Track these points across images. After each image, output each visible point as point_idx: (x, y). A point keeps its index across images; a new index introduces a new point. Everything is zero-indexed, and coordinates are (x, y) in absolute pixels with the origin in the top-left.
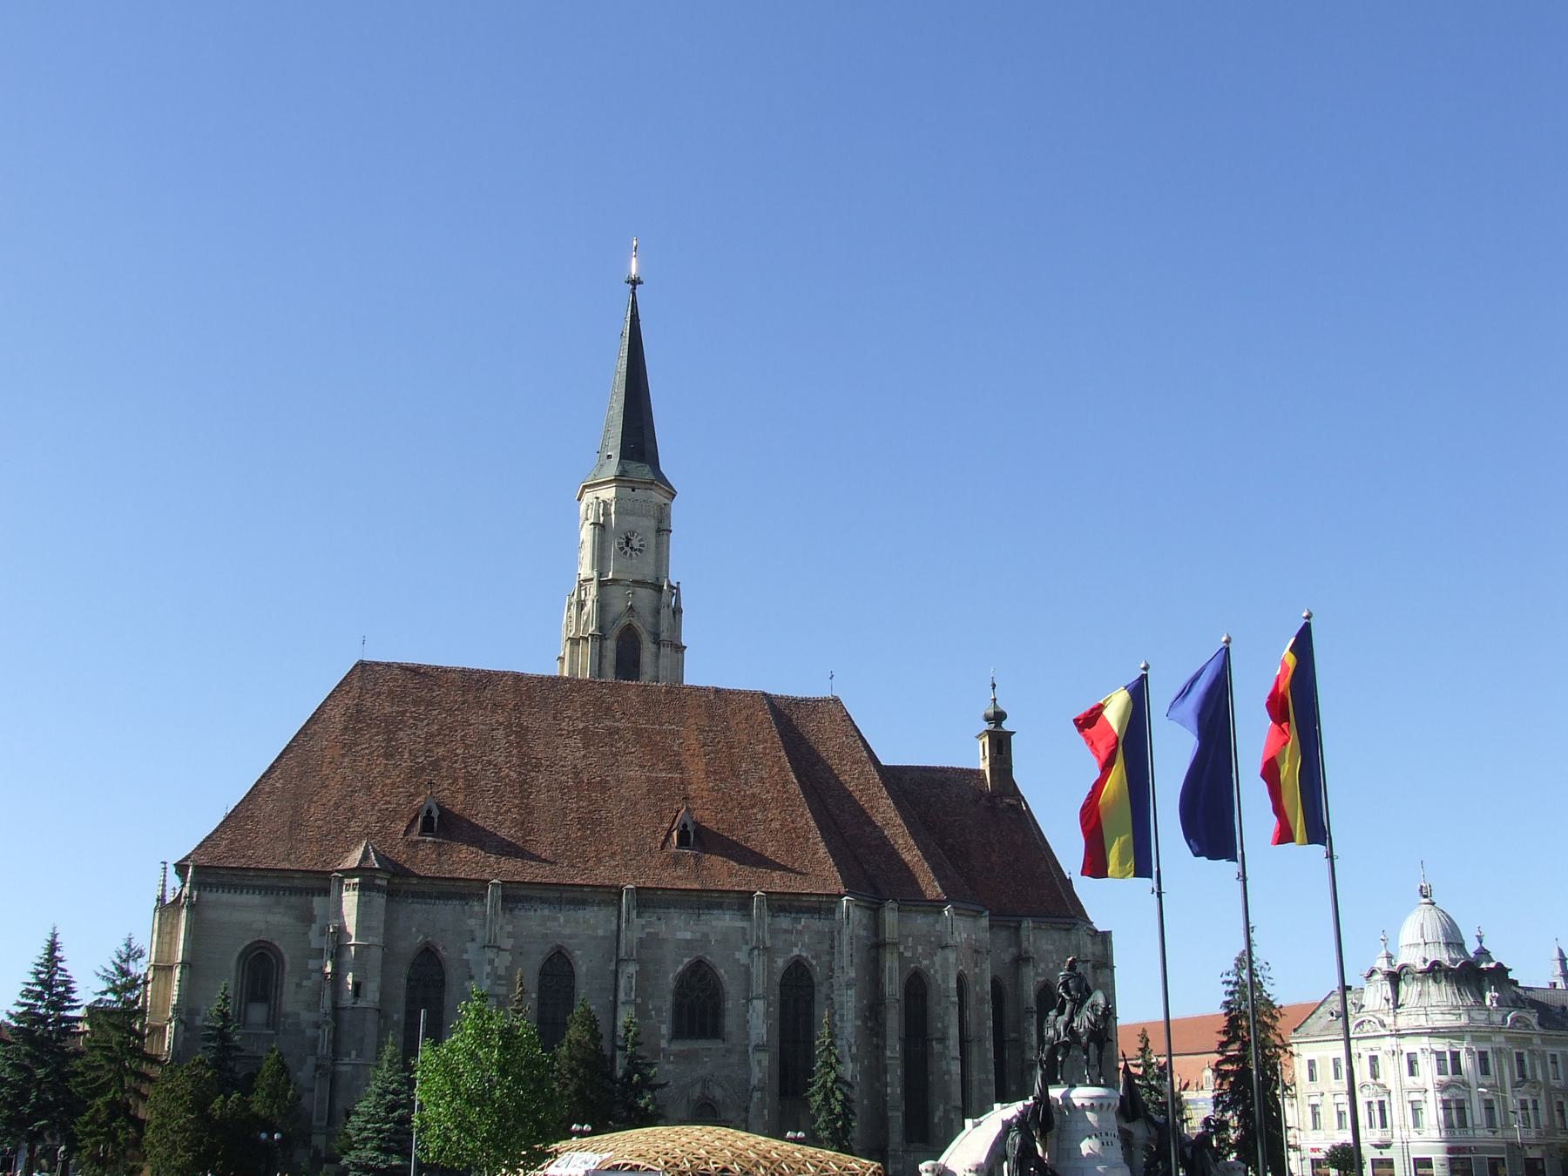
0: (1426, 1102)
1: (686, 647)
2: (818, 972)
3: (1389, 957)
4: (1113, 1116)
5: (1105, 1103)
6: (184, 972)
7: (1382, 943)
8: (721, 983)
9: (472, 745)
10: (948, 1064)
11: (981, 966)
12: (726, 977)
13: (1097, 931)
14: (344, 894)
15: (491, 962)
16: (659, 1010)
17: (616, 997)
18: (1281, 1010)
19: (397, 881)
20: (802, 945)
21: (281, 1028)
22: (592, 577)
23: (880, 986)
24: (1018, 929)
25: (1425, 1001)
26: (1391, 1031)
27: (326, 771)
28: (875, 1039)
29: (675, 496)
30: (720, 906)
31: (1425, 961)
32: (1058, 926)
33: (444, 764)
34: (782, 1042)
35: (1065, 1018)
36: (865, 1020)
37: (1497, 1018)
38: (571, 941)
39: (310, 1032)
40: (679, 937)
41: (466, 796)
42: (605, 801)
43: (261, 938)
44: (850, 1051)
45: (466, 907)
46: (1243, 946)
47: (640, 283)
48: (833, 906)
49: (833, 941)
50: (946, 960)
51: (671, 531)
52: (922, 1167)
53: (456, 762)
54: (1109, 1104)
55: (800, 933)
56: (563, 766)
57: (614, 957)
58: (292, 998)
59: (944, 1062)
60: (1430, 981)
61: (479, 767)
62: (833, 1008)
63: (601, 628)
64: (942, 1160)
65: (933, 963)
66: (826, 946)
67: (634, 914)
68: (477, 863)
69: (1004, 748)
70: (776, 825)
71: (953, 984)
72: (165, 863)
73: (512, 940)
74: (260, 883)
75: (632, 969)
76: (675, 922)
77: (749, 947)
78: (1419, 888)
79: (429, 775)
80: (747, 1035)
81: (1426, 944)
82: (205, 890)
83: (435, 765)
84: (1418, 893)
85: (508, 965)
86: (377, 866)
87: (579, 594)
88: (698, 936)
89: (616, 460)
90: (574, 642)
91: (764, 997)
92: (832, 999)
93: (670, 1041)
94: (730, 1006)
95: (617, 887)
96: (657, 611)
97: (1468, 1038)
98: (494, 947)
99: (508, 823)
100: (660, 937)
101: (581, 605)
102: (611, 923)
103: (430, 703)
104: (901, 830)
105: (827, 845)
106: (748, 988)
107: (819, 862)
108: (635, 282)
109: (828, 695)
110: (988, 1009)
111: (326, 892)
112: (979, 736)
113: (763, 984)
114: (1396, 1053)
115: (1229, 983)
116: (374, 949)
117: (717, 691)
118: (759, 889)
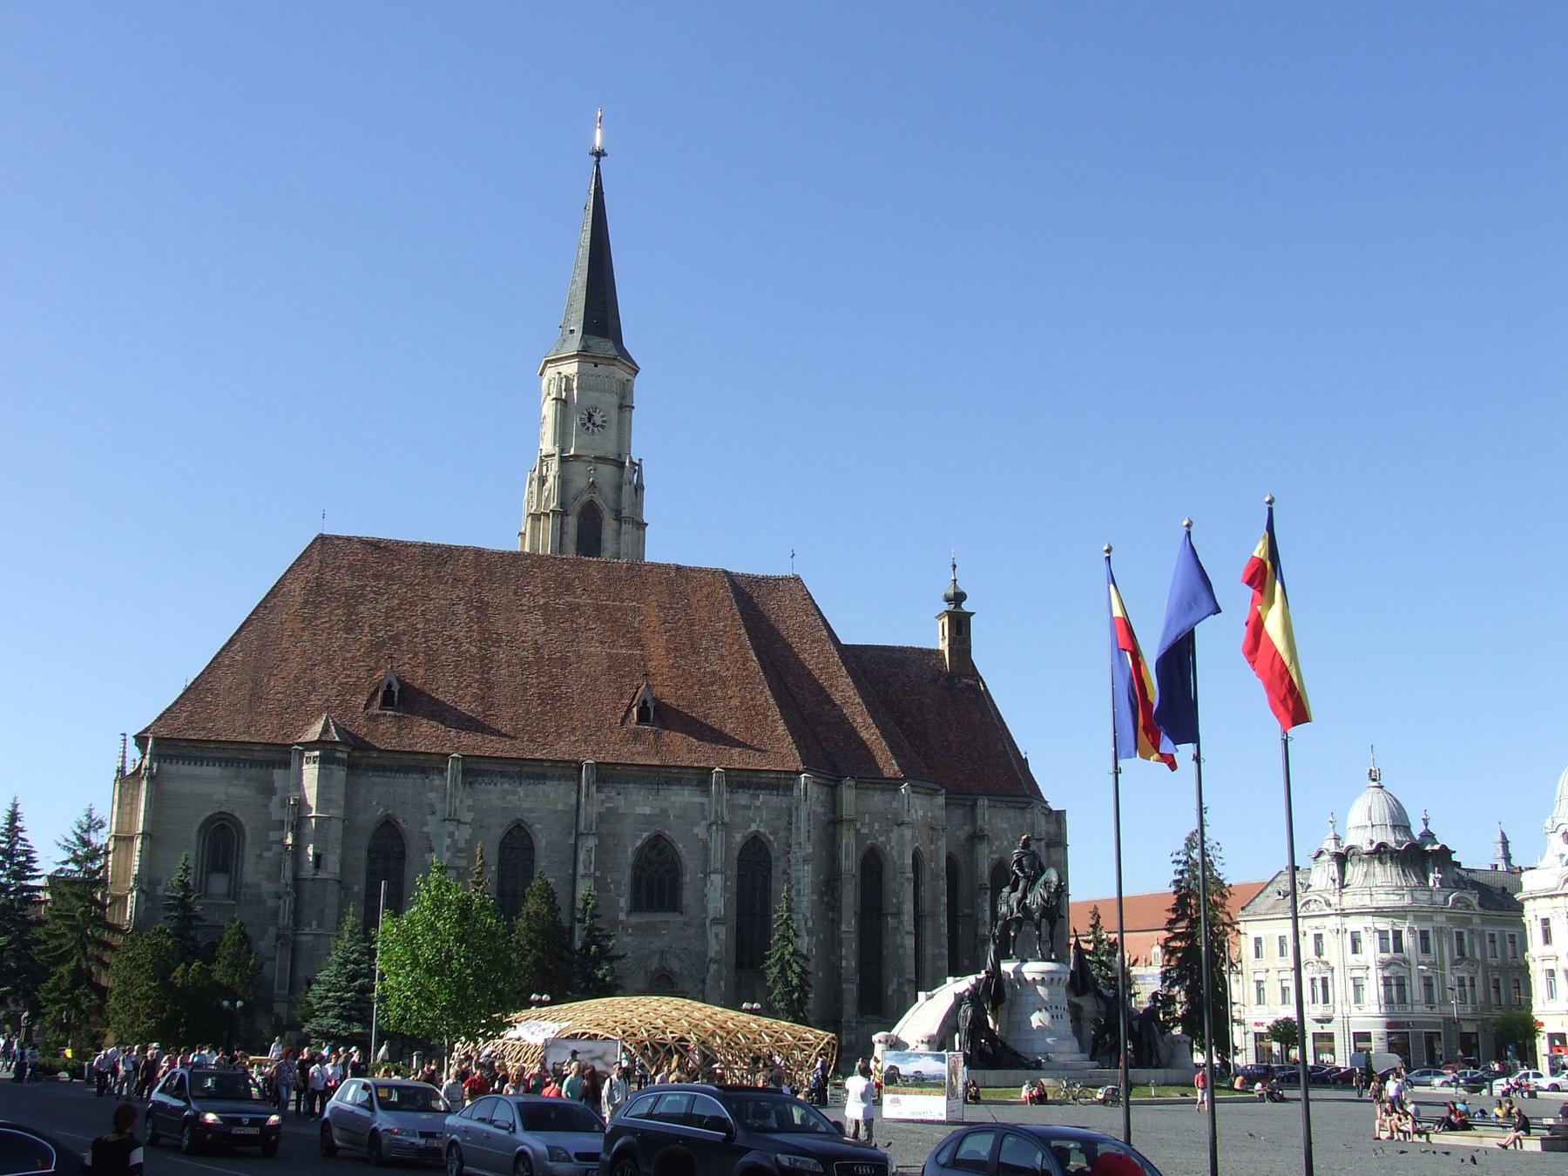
0: (1367, 979)
1: (647, 524)
2: (776, 847)
3: (1337, 839)
4: (1063, 991)
5: (1056, 977)
6: (145, 842)
7: (1331, 825)
8: (680, 859)
9: (432, 620)
10: (902, 938)
11: (937, 844)
12: (684, 850)
13: (1051, 810)
14: (305, 767)
15: (451, 835)
16: (617, 883)
17: (575, 870)
18: (1230, 889)
19: (357, 755)
20: (761, 821)
21: (242, 898)
22: (554, 452)
23: (837, 862)
24: (974, 807)
25: (1370, 882)
26: (1336, 910)
27: (286, 644)
28: (830, 913)
29: (638, 371)
30: (679, 782)
31: (1372, 842)
32: (1013, 804)
33: (405, 639)
34: (738, 915)
35: (1018, 894)
36: (821, 894)
37: (1439, 898)
38: (532, 815)
39: (271, 903)
40: (637, 812)
41: (427, 670)
42: (565, 677)
43: (223, 809)
44: (806, 924)
45: (427, 780)
46: (1195, 826)
47: (605, 155)
48: (791, 782)
49: (790, 817)
50: (902, 836)
51: (633, 408)
52: (875, 1038)
53: (416, 636)
54: (1060, 979)
55: (757, 808)
56: (523, 642)
57: (574, 832)
58: (252, 869)
59: (899, 937)
60: (1376, 862)
61: (439, 642)
62: (790, 883)
63: (562, 504)
64: (895, 1031)
65: (889, 839)
66: (783, 823)
67: (594, 788)
68: (437, 737)
69: (963, 629)
70: (735, 702)
71: (909, 861)
72: (124, 735)
73: (472, 814)
74: (220, 755)
75: (591, 842)
76: (634, 797)
77: (709, 822)
78: (1368, 772)
79: (389, 649)
80: (705, 907)
81: (1373, 826)
82: (165, 762)
83: (396, 638)
84: (1368, 777)
85: (468, 838)
86: (337, 739)
87: (541, 470)
88: (658, 811)
89: (578, 335)
90: (536, 517)
91: (721, 873)
92: (789, 874)
93: (629, 914)
94: (688, 880)
95: (576, 762)
96: (619, 488)
97: (1410, 917)
98: (454, 820)
99: (468, 698)
100: (620, 811)
101: (543, 480)
102: (571, 797)
103: (390, 578)
104: (860, 708)
105: (786, 722)
106: (706, 861)
107: (778, 739)
108: (599, 154)
109: (789, 574)
110: (943, 885)
111: (286, 764)
112: (939, 617)
113: (721, 858)
114: (1340, 932)
115: (1179, 862)
116: (334, 821)
117: (678, 568)
118: (718, 765)
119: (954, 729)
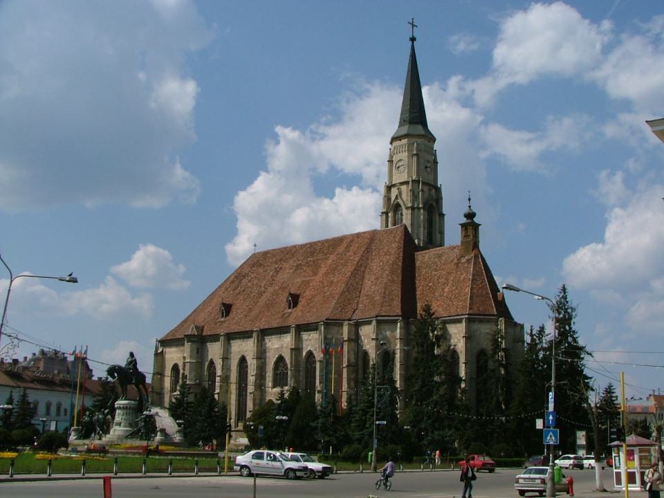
5: (129, 406)
16: (269, 377)
43: (175, 362)
55: (310, 340)
70: (328, 293)
76: (274, 341)
88: (280, 346)
119: (450, 284)
